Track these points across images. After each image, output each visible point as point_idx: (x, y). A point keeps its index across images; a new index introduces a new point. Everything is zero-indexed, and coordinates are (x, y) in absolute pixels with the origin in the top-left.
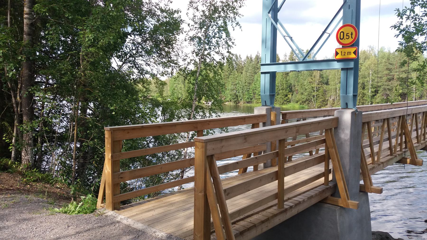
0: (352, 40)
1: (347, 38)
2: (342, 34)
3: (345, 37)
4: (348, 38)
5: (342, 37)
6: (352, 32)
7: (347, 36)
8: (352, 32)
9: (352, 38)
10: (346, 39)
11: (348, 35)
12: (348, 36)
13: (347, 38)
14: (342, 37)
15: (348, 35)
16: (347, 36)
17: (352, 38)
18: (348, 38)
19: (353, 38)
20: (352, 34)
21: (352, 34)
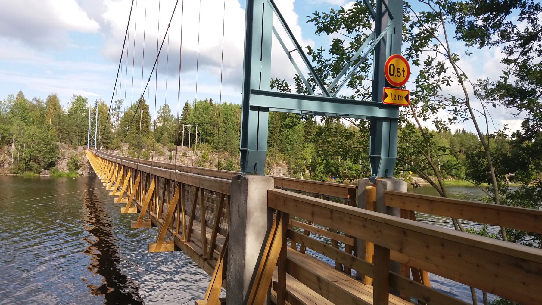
0: (404, 79)
1: (397, 75)
2: (392, 67)
3: (396, 73)
4: (399, 75)
5: (392, 73)
6: (404, 68)
7: (398, 72)
8: (404, 68)
9: (404, 77)
10: (396, 76)
11: (399, 70)
12: (400, 72)
13: (397, 75)
14: (392, 73)
15: (399, 70)
16: (398, 72)
17: (404, 77)
18: (399, 75)
19: (405, 77)
20: (403, 71)
21: (403, 71)
